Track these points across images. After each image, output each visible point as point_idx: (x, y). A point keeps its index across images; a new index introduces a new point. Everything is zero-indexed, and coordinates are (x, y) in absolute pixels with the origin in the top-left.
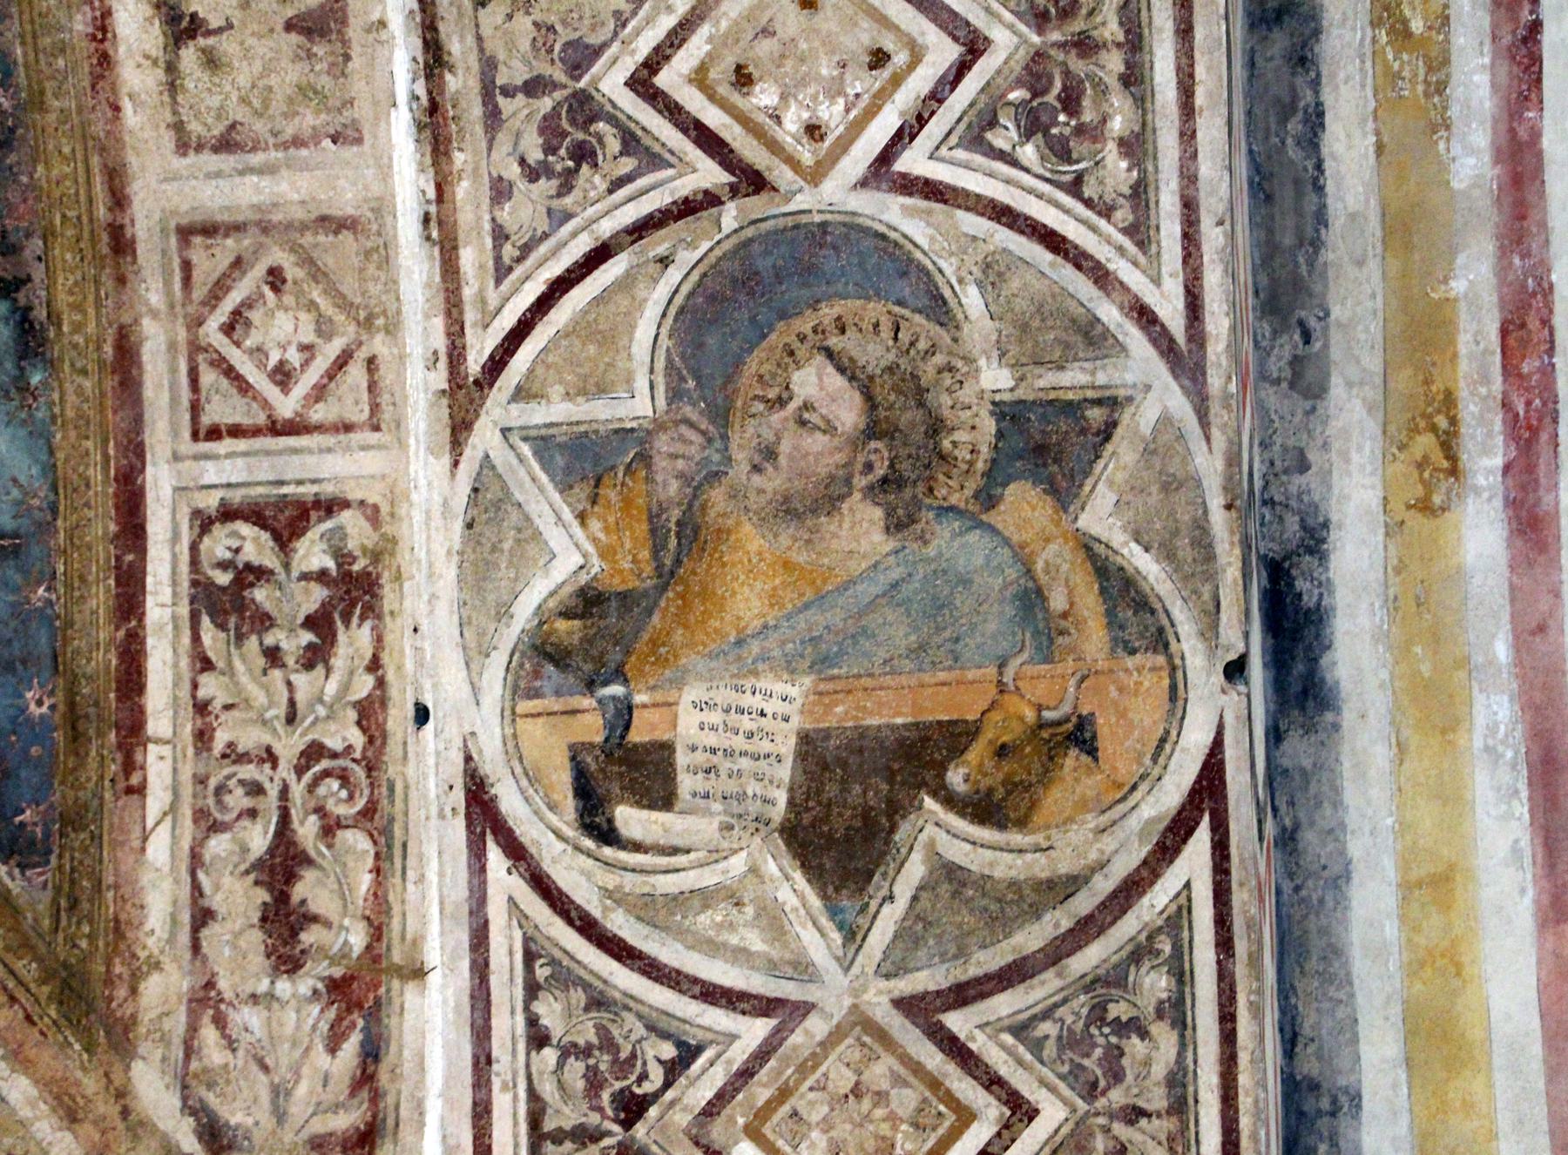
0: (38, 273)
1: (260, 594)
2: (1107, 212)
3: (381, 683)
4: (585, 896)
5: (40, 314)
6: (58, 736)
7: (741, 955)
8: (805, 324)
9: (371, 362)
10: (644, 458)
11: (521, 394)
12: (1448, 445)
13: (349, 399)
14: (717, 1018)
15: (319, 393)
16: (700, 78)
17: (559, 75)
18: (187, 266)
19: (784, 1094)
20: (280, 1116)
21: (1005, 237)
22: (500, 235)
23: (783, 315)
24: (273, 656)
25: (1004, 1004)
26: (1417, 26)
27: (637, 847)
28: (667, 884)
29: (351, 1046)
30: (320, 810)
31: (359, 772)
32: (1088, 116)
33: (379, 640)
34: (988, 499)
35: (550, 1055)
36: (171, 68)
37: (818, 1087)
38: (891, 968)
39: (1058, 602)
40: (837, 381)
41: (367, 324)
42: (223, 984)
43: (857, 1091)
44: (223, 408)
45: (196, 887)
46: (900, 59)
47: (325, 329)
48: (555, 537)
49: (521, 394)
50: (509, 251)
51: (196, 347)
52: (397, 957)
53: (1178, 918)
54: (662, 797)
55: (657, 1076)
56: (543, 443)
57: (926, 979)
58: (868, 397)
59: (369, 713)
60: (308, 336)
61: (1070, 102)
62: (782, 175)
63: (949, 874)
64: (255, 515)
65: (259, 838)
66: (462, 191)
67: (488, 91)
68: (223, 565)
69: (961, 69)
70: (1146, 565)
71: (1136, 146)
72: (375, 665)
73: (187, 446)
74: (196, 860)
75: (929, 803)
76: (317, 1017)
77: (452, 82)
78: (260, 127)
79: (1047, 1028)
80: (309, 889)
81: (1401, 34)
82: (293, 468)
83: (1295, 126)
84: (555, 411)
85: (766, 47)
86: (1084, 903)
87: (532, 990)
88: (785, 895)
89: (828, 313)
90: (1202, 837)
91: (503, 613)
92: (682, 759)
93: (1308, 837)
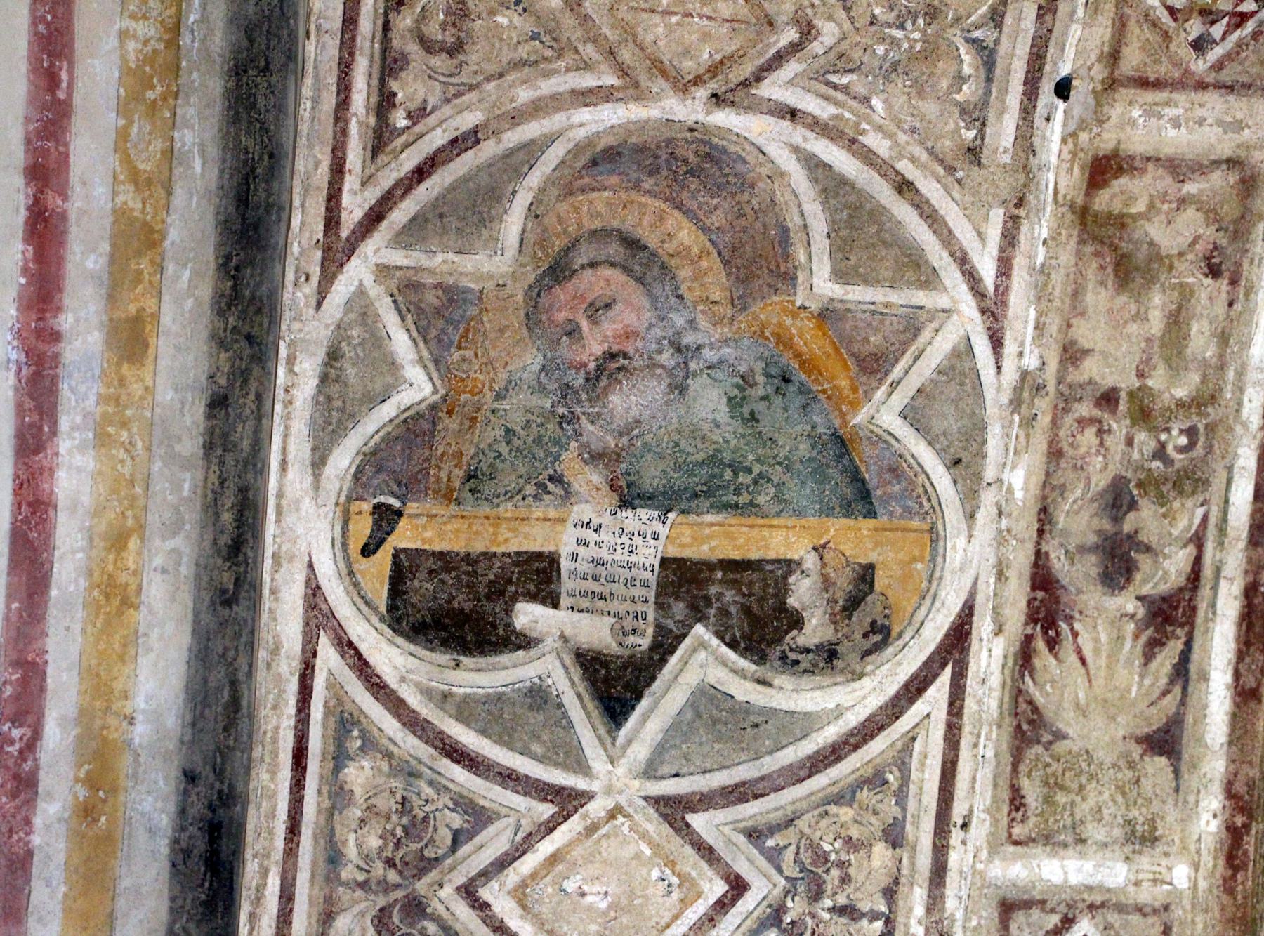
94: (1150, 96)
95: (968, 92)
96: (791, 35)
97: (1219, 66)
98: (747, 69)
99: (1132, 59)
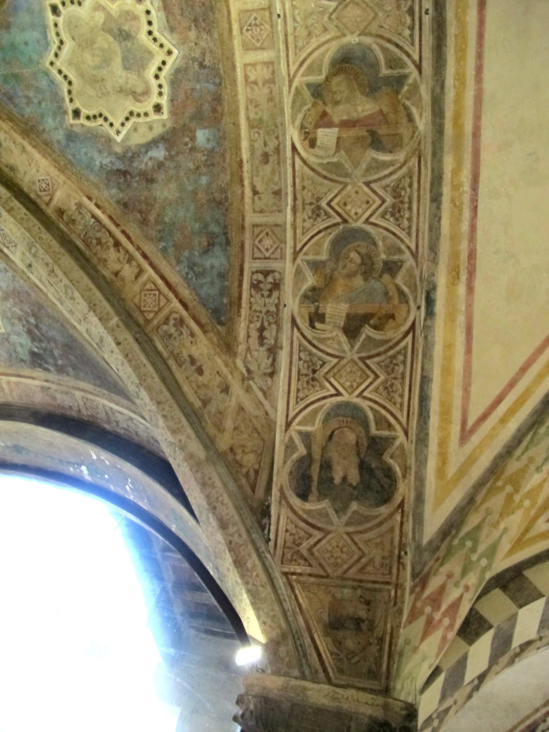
0: (230, 232)
1: (261, 285)
2: (404, 230)
3: (279, 301)
4: (309, 337)
5: (230, 238)
6: (228, 306)
7: (334, 348)
8: (353, 245)
9: (282, 249)
10: (324, 266)
11: (306, 254)
12: (458, 274)
13: (278, 254)
14: (329, 358)
15: (273, 253)
16: (338, 204)
17: (315, 202)
18: (253, 232)
19: (339, 371)
20: (259, 369)
21: (386, 233)
22: (303, 228)
23: (349, 243)
24: (263, 295)
25: (377, 359)
26: (458, 204)
27: (318, 329)
28: (323, 336)
29: (271, 359)
30: (268, 321)
31: (275, 316)
32: (402, 214)
33: (280, 294)
34: (380, 276)
35: (302, 362)
36: (253, 199)
37: (345, 370)
38: (358, 352)
39: (391, 294)
40: (357, 255)
41: (281, 242)
42: (251, 348)
43: (351, 372)
44: (257, 255)
45: (248, 332)
46: (371, 202)
47: (274, 242)
48: (309, 278)
49: (306, 254)
50: (305, 230)
51: (254, 245)
52: (279, 345)
53: (406, 348)
54: (323, 321)
55: (319, 366)
56: (308, 262)
57: (364, 354)
58: (362, 258)
59: (277, 306)
60: (272, 243)
61: (399, 211)
62: (350, 220)
63: (369, 338)
64: (261, 272)
65: (258, 325)
66: (298, 220)
67: (304, 204)
68: (256, 280)
69: (381, 205)
70: (406, 289)
71: (410, 219)
72: (279, 298)
73: (251, 260)
74: (248, 328)
75: (367, 326)
76: (266, 354)
77: (298, 202)
78: (266, 209)
79: (383, 364)
80: (266, 334)
81: (455, 205)
82: (268, 265)
83: (437, 219)
84: (310, 257)
85: (349, 199)
86: (390, 344)
87: (300, 351)
88: (342, 339)
89: (356, 244)
90: (410, 336)
91: (299, 290)
92: (327, 316)
93: (429, 337)
94: (260, 7)
95: (297, 12)
96: (333, 17)
97: (251, 15)
98: (340, 7)
99: (267, 14)
